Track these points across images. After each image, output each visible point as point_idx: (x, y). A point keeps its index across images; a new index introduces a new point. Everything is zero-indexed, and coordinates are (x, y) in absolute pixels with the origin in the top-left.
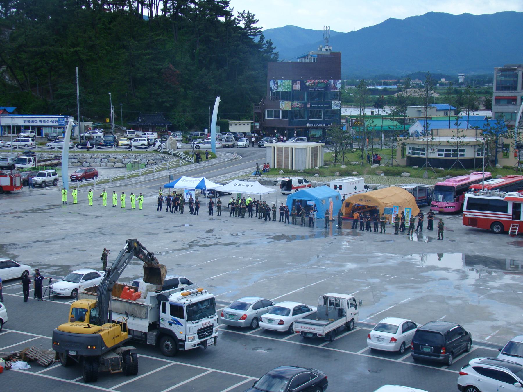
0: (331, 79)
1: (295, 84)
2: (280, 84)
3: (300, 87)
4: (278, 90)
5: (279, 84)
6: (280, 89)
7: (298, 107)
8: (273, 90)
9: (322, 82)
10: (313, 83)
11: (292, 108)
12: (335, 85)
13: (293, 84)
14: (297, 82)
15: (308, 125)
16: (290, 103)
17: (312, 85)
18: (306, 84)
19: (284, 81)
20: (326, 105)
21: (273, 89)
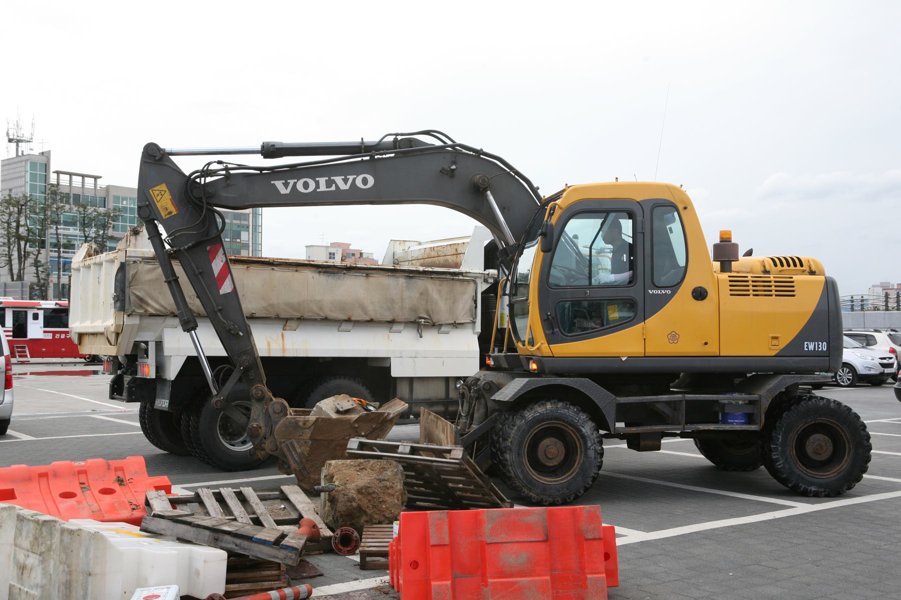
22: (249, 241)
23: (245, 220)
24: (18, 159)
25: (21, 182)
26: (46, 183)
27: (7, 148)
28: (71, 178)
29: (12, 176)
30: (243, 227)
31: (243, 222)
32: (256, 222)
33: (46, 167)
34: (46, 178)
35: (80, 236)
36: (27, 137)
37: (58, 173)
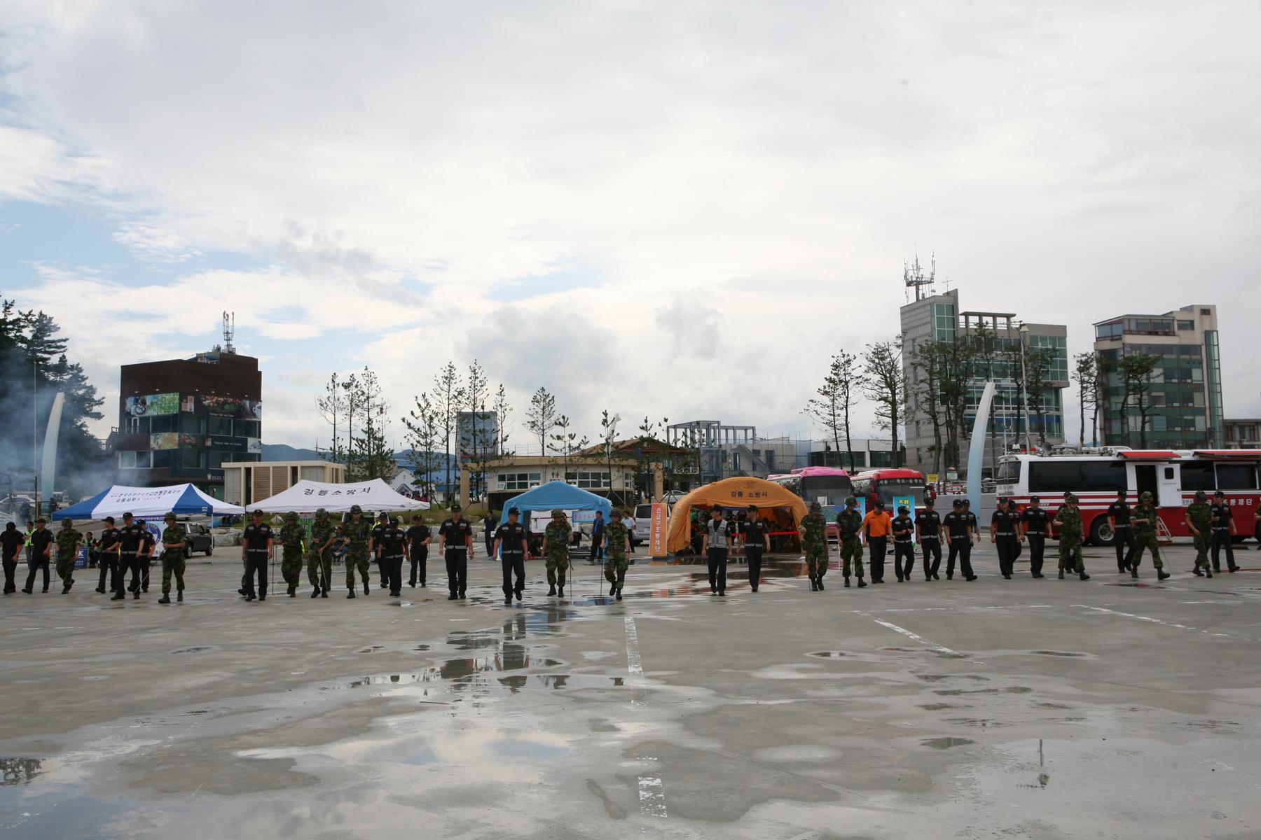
0: (247, 399)
1: (185, 400)
2: (152, 404)
3: (193, 407)
4: (147, 415)
5: (148, 403)
6: (152, 412)
7: (190, 444)
8: (134, 416)
9: (231, 403)
10: (216, 402)
11: (180, 445)
12: (251, 410)
13: (181, 400)
14: (189, 397)
15: (209, 477)
16: (176, 436)
17: (215, 405)
18: (204, 402)
19: (160, 396)
20: (238, 444)
21: (132, 413)
22: (1203, 381)
23: (1196, 354)
24: (920, 304)
25: (927, 329)
26: (954, 328)
27: (906, 293)
28: (980, 319)
29: (914, 324)
30: (1194, 363)
31: (1194, 357)
32: (1210, 356)
33: (954, 308)
34: (954, 322)
35: (1012, 388)
36: (927, 276)
37: (967, 315)
